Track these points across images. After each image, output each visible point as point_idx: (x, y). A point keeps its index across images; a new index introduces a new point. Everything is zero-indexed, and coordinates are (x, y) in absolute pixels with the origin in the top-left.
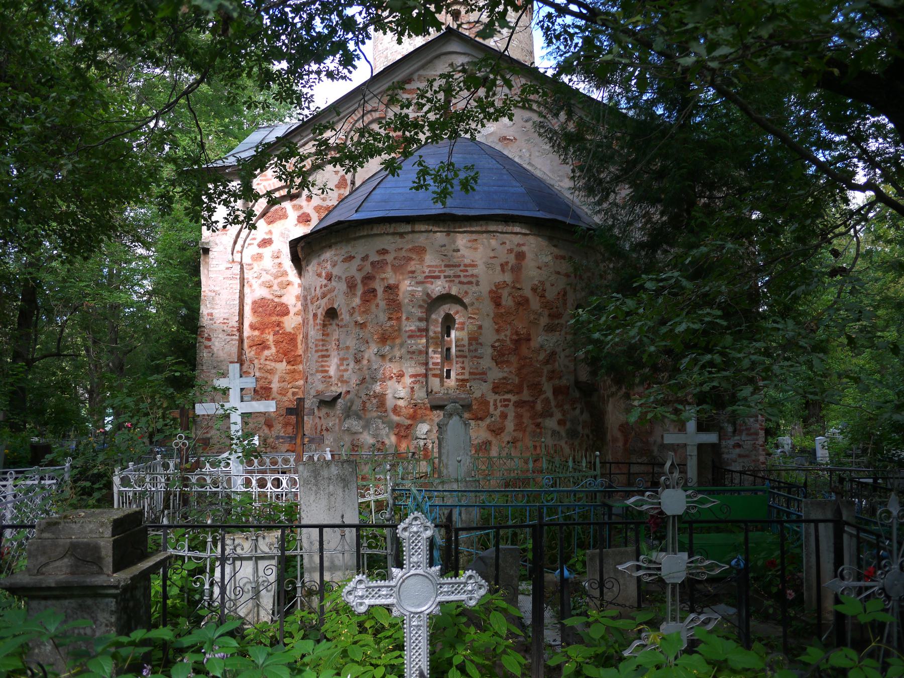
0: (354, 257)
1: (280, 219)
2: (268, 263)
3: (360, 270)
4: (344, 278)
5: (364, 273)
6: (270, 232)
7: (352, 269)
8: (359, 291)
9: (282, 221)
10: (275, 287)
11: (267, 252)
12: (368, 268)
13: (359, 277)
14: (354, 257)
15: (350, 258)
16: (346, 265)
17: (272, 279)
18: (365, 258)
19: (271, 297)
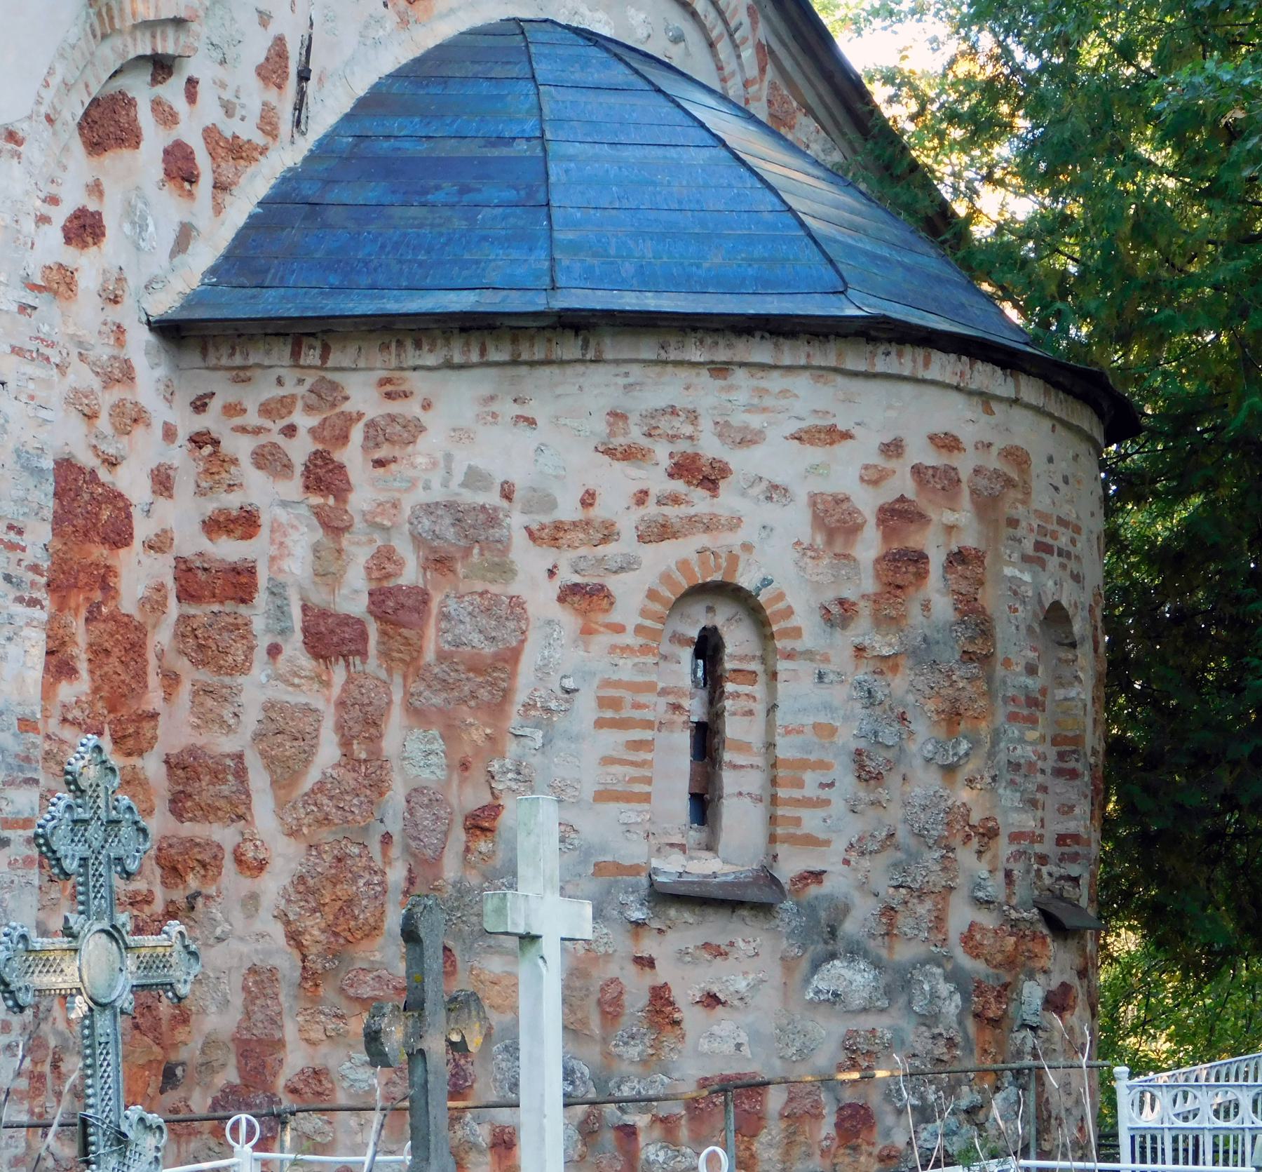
0: (847, 436)
1: (121, 142)
2: (86, 313)
3: (875, 483)
4: (802, 498)
5: (887, 494)
6: (96, 189)
7: (843, 473)
8: (869, 546)
9: (126, 153)
10: (104, 423)
11: (90, 266)
12: (902, 484)
13: (867, 503)
14: (847, 436)
15: (834, 435)
16: (815, 454)
17: (96, 383)
18: (893, 448)
19: (87, 459)
